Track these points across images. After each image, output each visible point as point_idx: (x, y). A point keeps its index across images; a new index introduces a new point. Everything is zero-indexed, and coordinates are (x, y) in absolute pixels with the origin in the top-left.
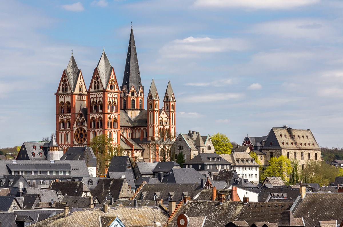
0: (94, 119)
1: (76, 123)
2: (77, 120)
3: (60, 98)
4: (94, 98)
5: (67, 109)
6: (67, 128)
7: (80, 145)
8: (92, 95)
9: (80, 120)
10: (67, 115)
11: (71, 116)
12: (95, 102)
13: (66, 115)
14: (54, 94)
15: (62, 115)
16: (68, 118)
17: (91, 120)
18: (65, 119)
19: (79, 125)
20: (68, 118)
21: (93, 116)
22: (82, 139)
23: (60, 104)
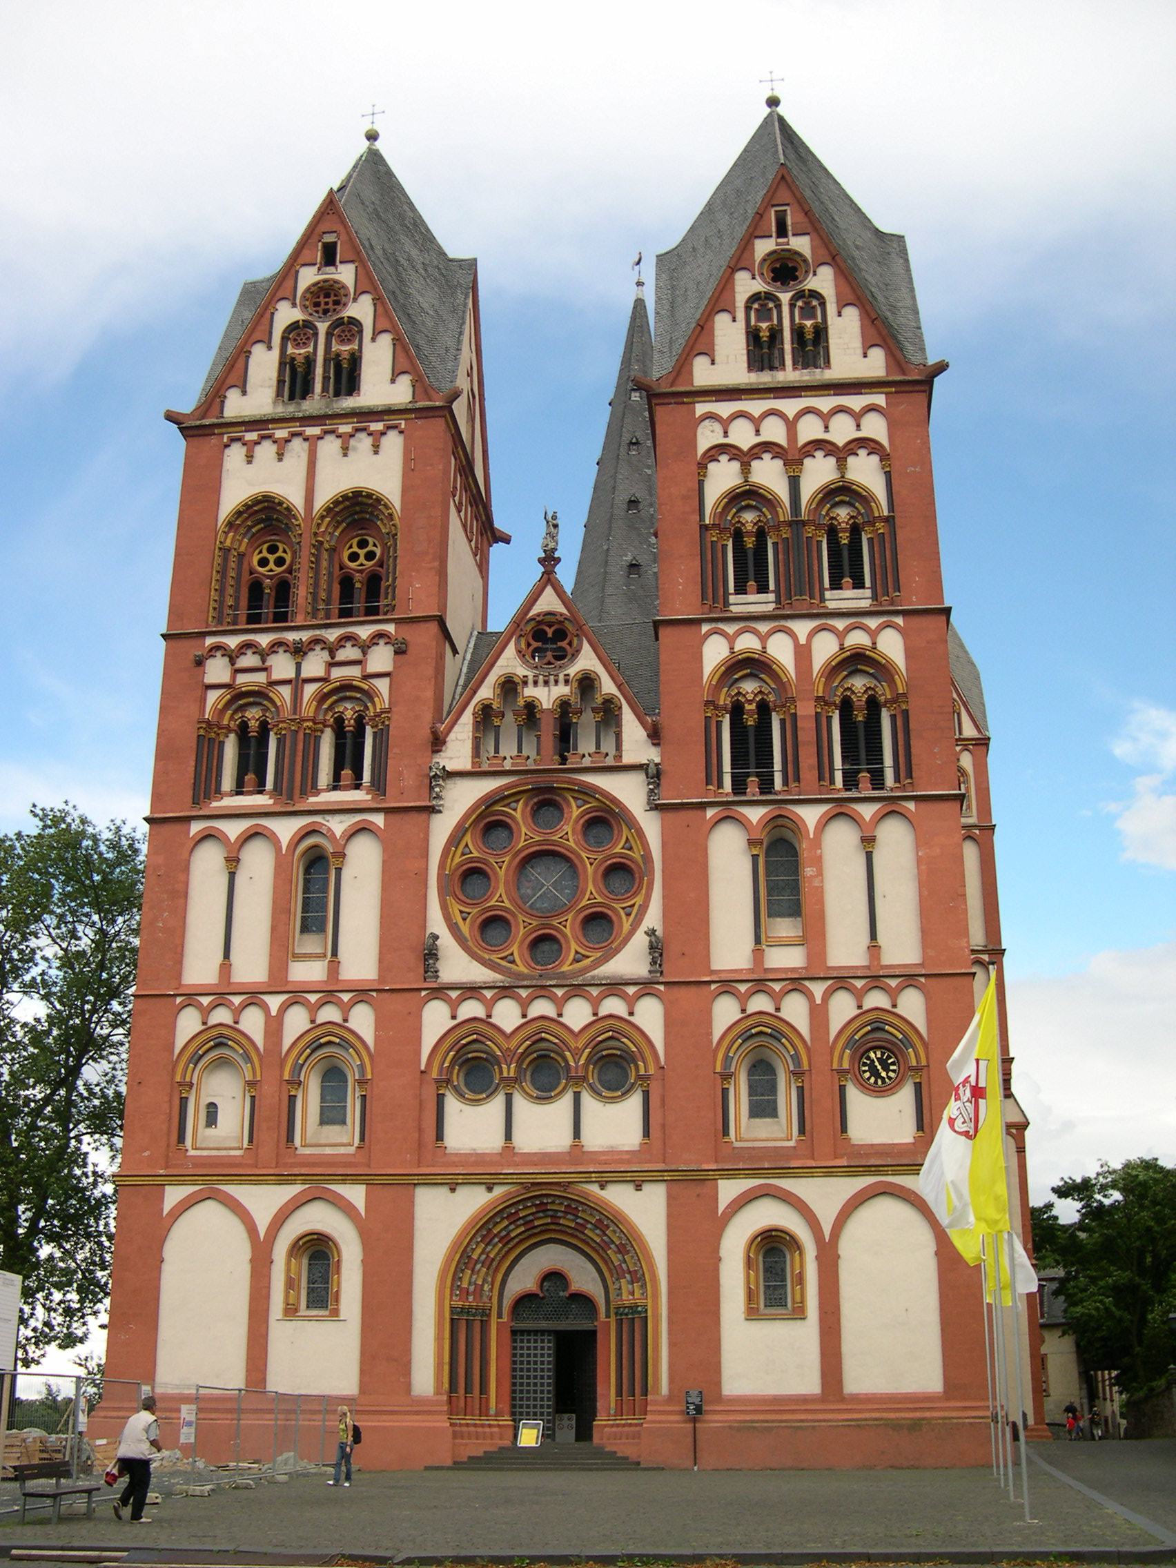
2: (486, 692)
3: (250, 458)
4: (745, 458)
6: (317, 792)
7: (542, 991)
8: (725, 424)
9: (546, 696)
10: (332, 635)
13: (316, 641)
14: (171, 417)
15: (264, 640)
16: (337, 673)
18: (298, 683)
19: (509, 749)
20: (355, 672)
21: (748, 643)
22: (569, 927)
23: (230, 525)
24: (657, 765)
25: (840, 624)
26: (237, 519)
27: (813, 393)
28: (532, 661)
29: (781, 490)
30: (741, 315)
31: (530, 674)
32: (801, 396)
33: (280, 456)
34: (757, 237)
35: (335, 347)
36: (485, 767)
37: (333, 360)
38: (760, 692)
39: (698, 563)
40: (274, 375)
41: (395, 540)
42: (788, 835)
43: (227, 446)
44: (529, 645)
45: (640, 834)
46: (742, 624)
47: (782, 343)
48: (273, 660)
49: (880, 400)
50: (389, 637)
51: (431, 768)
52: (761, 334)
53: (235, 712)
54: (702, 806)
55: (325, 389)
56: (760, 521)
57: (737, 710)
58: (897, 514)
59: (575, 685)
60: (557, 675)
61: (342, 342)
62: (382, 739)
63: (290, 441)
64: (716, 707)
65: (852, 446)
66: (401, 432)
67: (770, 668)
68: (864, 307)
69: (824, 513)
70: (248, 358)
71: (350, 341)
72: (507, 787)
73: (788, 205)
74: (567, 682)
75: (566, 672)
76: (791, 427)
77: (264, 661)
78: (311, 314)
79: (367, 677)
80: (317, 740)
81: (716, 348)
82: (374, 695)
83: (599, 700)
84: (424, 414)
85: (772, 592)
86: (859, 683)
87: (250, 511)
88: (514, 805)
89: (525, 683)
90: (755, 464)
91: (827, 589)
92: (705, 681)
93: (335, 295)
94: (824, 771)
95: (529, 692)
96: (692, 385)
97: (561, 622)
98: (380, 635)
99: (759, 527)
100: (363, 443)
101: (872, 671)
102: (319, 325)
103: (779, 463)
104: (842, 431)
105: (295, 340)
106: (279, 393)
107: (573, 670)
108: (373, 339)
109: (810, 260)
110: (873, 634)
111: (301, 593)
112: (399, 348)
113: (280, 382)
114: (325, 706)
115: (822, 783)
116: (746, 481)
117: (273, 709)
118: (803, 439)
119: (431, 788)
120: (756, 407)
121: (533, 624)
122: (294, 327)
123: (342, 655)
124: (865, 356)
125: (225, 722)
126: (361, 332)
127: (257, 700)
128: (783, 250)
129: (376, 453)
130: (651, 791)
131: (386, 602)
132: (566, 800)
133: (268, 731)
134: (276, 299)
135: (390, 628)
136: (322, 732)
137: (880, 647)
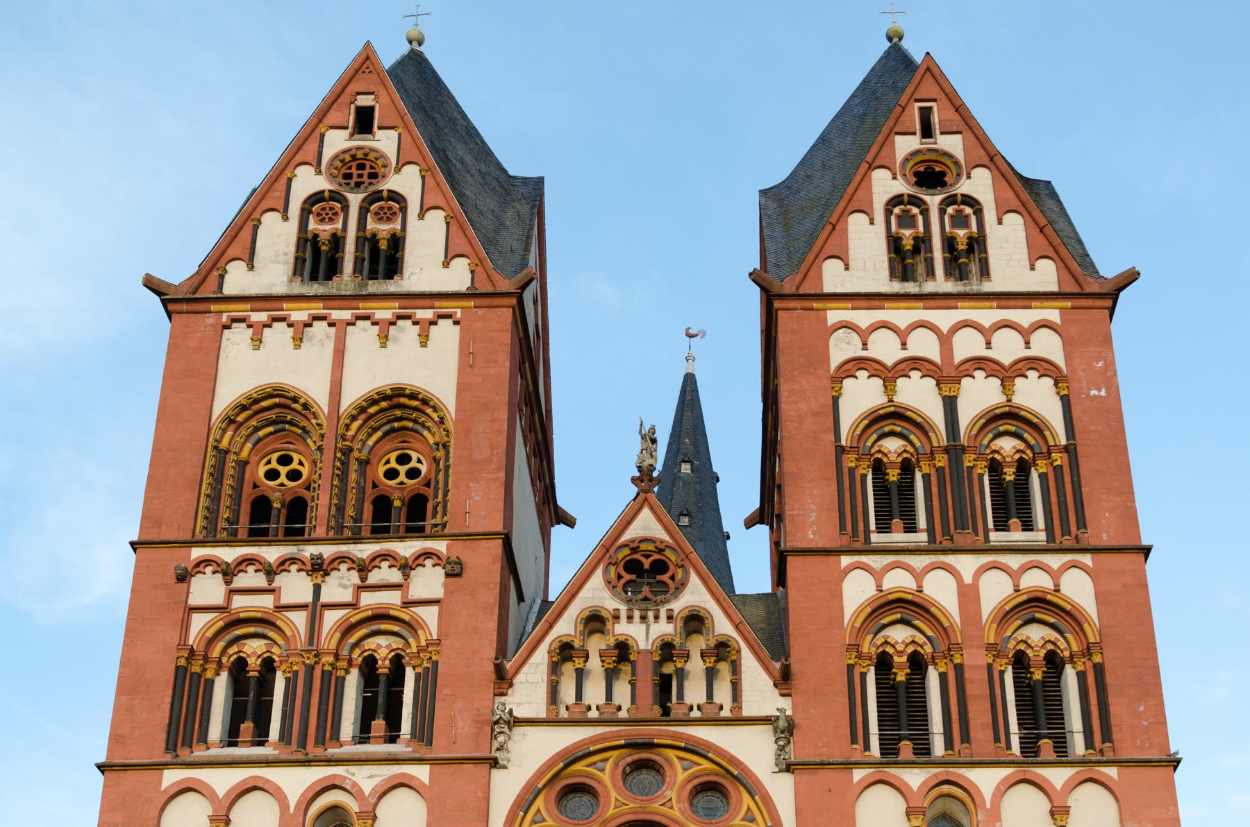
0: (899, 635)
1: (555, 668)
2: (566, 627)
3: (257, 341)
4: (889, 375)
5: (352, 496)
8: (864, 335)
10: (364, 551)
11: (454, 571)
12: (922, 427)
13: (342, 558)
16: (368, 599)
17: (861, 631)
18: (316, 609)
19: (594, 693)
20: (394, 598)
21: (899, 581)
23: (231, 421)
24: (789, 720)
25: (1014, 561)
26: (238, 414)
27: (972, 304)
28: (623, 594)
29: (935, 414)
30: (879, 216)
31: (623, 609)
32: (956, 308)
33: (298, 341)
34: (897, 133)
35: (371, 225)
36: (564, 714)
37: (368, 242)
38: (913, 642)
39: (833, 488)
40: (292, 249)
41: (448, 453)
42: (954, 808)
43: (227, 327)
44: (620, 577)
45: (768, 801)
46: (891, 558)
47: (931, 250)
48: (281, 580)
49: (1053, 315)
50: (439, 558)
51: (493, 712)
52: (904, 242)
53: (230, 644)
54: (849, 765)
55: (357, 269)
56: (905, 451)
57: (883, 663)
58: (1079, 442)
59: (680, 624)
60: (658, 610)
61: (380, 220)
62: (427, 682)
63: (310, 325)
64: (859, 656)
65: (1020, 365)
66: (456, 323)
67: (927, 611)
68: (1030, 214)
69: (985, 442)
70: (256, 228)
71: (389, 220)
72: (594, 740)
73: (934, 100)
74: (670, 618)
75: (669, 607)
76: (945, 340)
77: (270, 581)
78: (341, 185)
79: (407, 604)
80: (341, 682)
81: (851, 252)
82: (416, 626)
83: (712, 643)
84: (487, 301)
85: (922, 531)
86: (1036, 634)
87: (255, 407)
88: (600, 765)
89: (616, 617)
90: (901, 382)
91: (991, 530)
92: (846, 622)
93: (372, 167)
94: (999, 732)
95: (623, 629)
96: (822, 290)
97: (660, 551)
98: (428, 554)
99: (905, 459)
100: (407, 331)
101: (1052, 620)
102: (350, 196)
103: (931, 382)
104: (1007, 348)
105: (319, 214)
106: (298, 270)
107: (679, 605)
108: (421, 216)
109: (963, 162)
110: (1055, 575)
111: (321, 505)
112: (454, 228)
113: (299, 262)
114: (352, 640)
115: (998, 745)
116: (890, 401)
117: (281, 642)
118: (959, 356)
119: (493, 737)
120: (902, 316)
121: (626, 551)
122: (316, 198)
123: (374, 577)
124: (1033, 269)
125: (216, 653)
126: (404, 210)
127: (260, 630)
128: (929, 150)
129: (424, 344)
130: (781, 749)
131: (433, 521)
132: (667, 760)
133: (273, 671)
134: (294, 163)
135: (441, 546)
136: (347, 672)
137: (1065, 590)
